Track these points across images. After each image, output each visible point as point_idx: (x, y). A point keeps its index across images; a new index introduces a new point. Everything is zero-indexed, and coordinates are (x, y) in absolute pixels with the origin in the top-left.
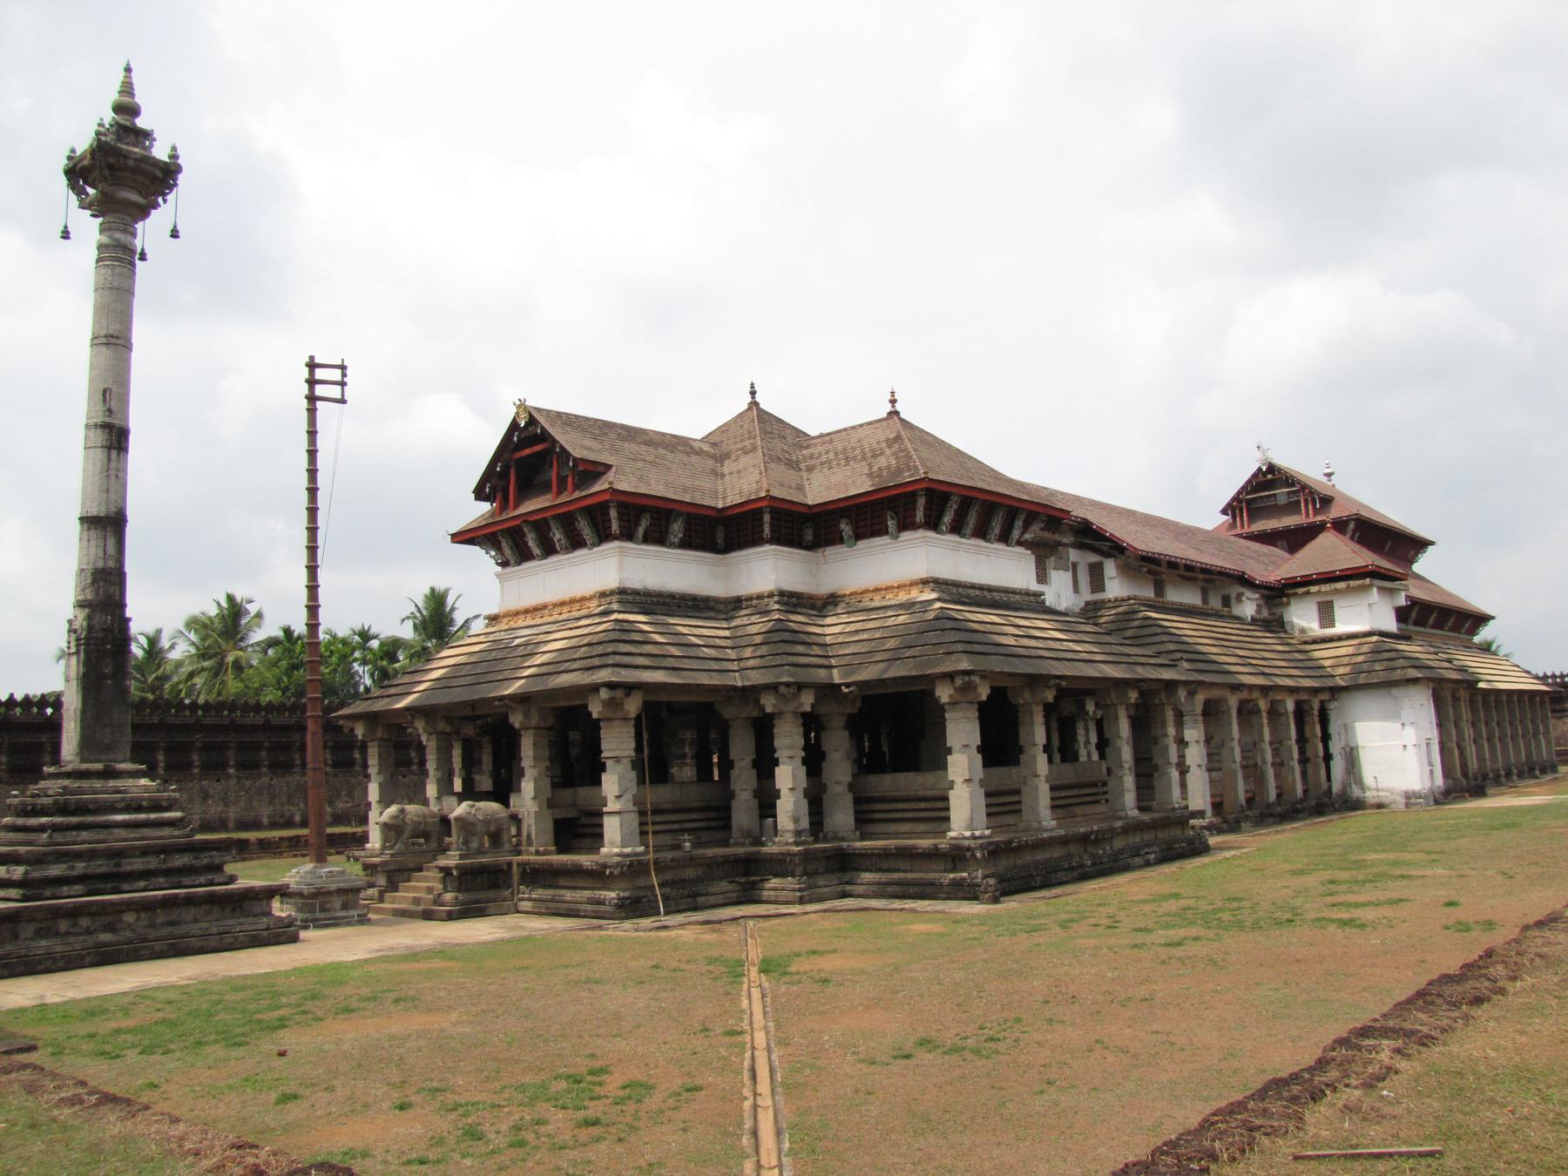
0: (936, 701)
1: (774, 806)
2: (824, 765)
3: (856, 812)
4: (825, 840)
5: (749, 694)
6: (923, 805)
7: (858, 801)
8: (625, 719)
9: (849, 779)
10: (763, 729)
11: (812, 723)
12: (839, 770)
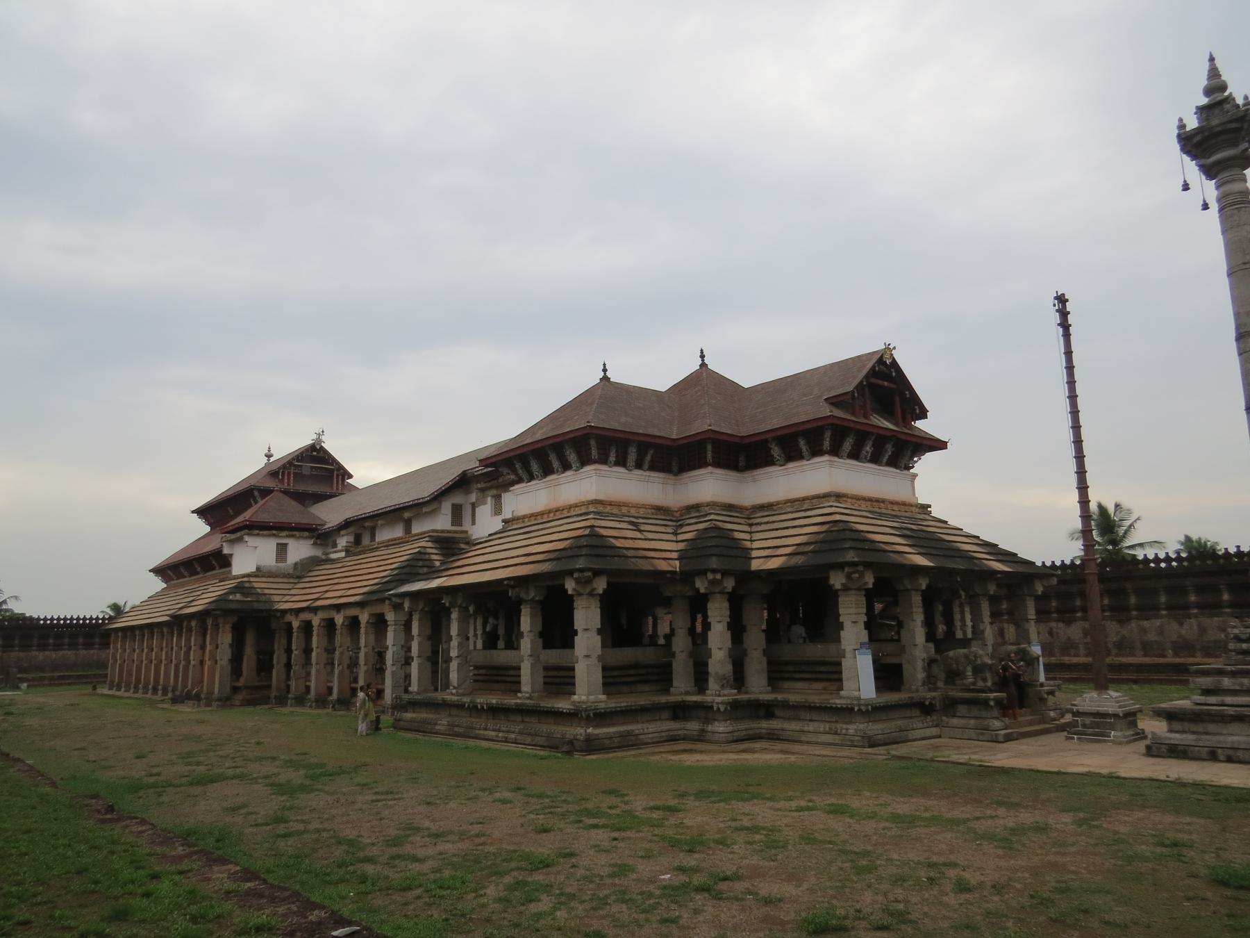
0: (831, 587)
1: (706, 665)
2: (745, 635)
3: (769, 672)
4: (746, 693)
5: (686, 577)
6: (822, 669)
7: (769, 663)
8: (591, 594)
9: (763, 644)
10: (698, 604)
11: (736, 603)
12: (755, 640)
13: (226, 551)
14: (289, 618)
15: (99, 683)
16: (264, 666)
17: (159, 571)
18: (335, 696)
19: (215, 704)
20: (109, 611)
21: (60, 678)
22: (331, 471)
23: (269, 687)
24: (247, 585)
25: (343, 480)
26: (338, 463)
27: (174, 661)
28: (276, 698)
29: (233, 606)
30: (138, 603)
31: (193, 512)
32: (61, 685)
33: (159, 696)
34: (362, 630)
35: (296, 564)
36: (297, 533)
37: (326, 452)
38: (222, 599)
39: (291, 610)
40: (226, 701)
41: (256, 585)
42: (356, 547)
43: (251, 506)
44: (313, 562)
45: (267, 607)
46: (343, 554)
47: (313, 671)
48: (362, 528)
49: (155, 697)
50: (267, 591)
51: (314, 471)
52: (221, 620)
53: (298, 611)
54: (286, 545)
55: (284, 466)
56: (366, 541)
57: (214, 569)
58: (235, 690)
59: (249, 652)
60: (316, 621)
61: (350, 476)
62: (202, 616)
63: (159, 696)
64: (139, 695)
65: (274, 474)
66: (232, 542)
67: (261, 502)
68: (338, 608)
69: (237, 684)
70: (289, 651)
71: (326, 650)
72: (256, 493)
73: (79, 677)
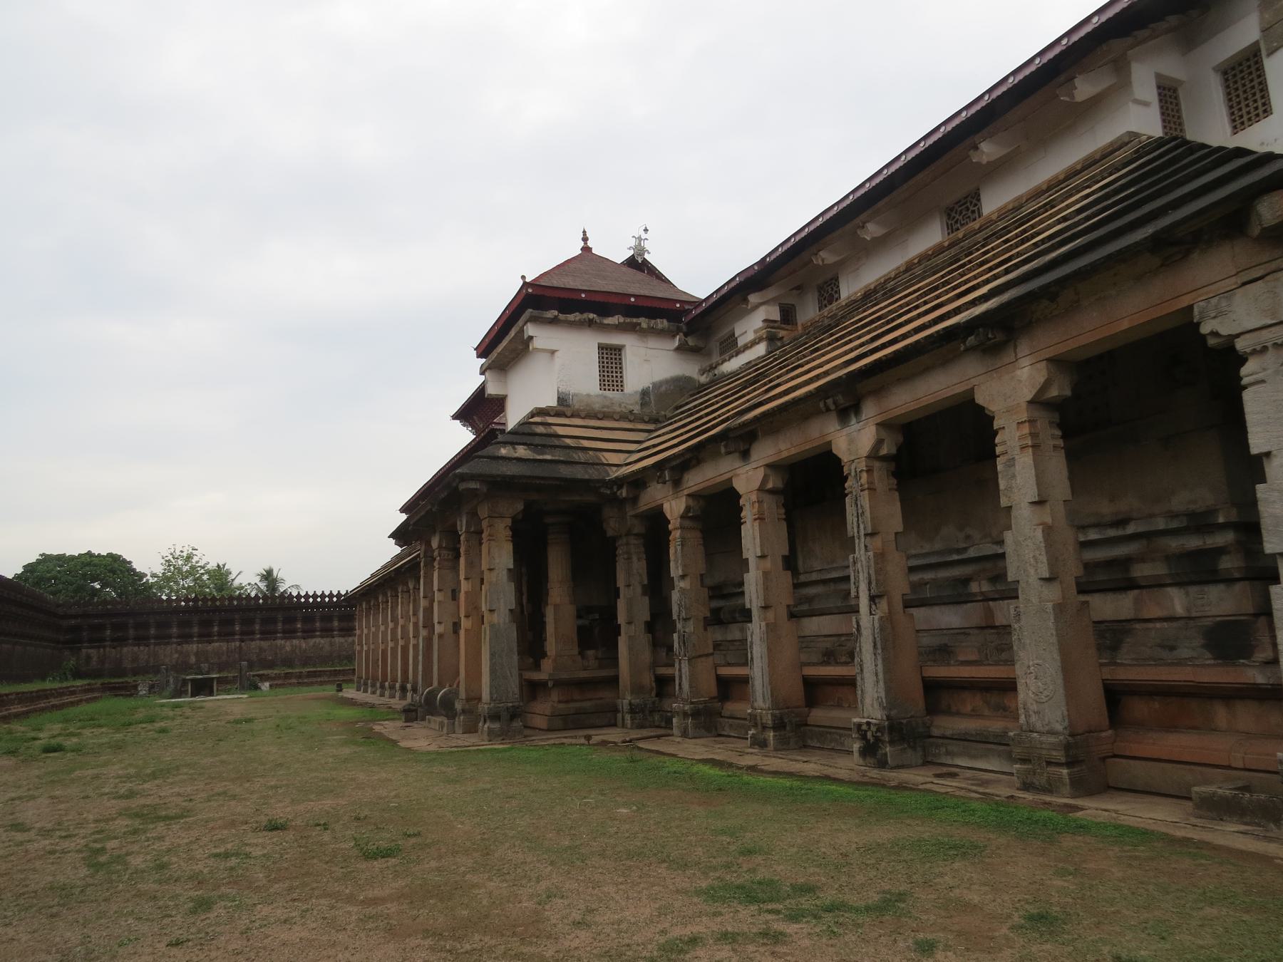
23: (613, 681)
24: (540, 430)
28: (633, 710)
40: (510, 720)
41: (560, 431)
45: (592, 474)
50: (586, 444)
52: (483, 511)
58: (533, 689)
59: (559, 594)
69: (535, 676)
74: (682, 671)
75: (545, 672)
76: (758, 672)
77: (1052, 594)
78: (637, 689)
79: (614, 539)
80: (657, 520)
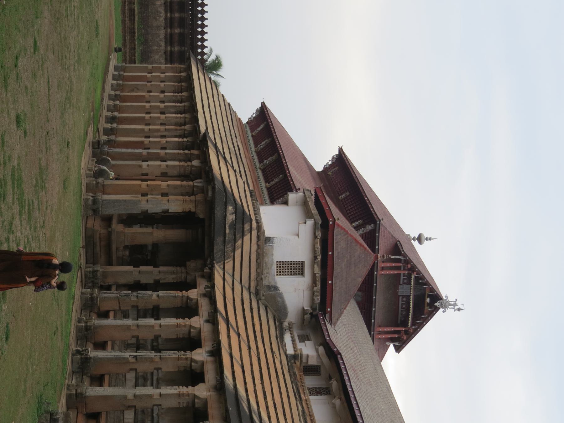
13: (292, 197)
14: (202, 284)
15: (124, 55)
16: (139, 255)
17: (263, 114)
18: (93, 353)
19: (93, 181)
20: (210, 60)
21: (132, 11)
22: (404, 323)
23: (110, 263)
24: (247, 227)
25: (392, 340)
26: (416, 332)
27: (146, 141)
28: (94, 272)
29: (218, 211)
30: (222, 90)
31: (341, 150)
32: (123, 12)
33: (103, 125)
34: (184, 390)
35: (276, 288)
36: (318, 288)
37: (431, 314)
38: (227, 197)
39: (213, 287)
40: (92, 209)
41: (247, 238)
42: (301, 368)
43: (351, 222)
44: (278, 310)
46: (290, 351)
47: (129, 322)
48: (331, 377)
49: (102, 120)
50: (238, 252)
51: (404, 301)
52: (199, 197)
53: (211, 296)
54: (302, 273)
55: (408, 261)
56: (310, 382)
57: (267, 180)
60: (198, 322)
61: (398, 349)
62: (206, 172)
63: (103, 125)
64: (107, 102)
65: (396, 249)
66: (305, 203)
67: (357, 235)
68: (216, 353)
69: (114, 221)
70: (157, 286)
71: (157, 337)
72: (369, 227)
73: (132, 33)
74: (113, 294)
75: (117, 227)
76: (110, 321)
77: (130, 396)
78: (105, 275)
79: (185, 266)
80: (195, 287)
